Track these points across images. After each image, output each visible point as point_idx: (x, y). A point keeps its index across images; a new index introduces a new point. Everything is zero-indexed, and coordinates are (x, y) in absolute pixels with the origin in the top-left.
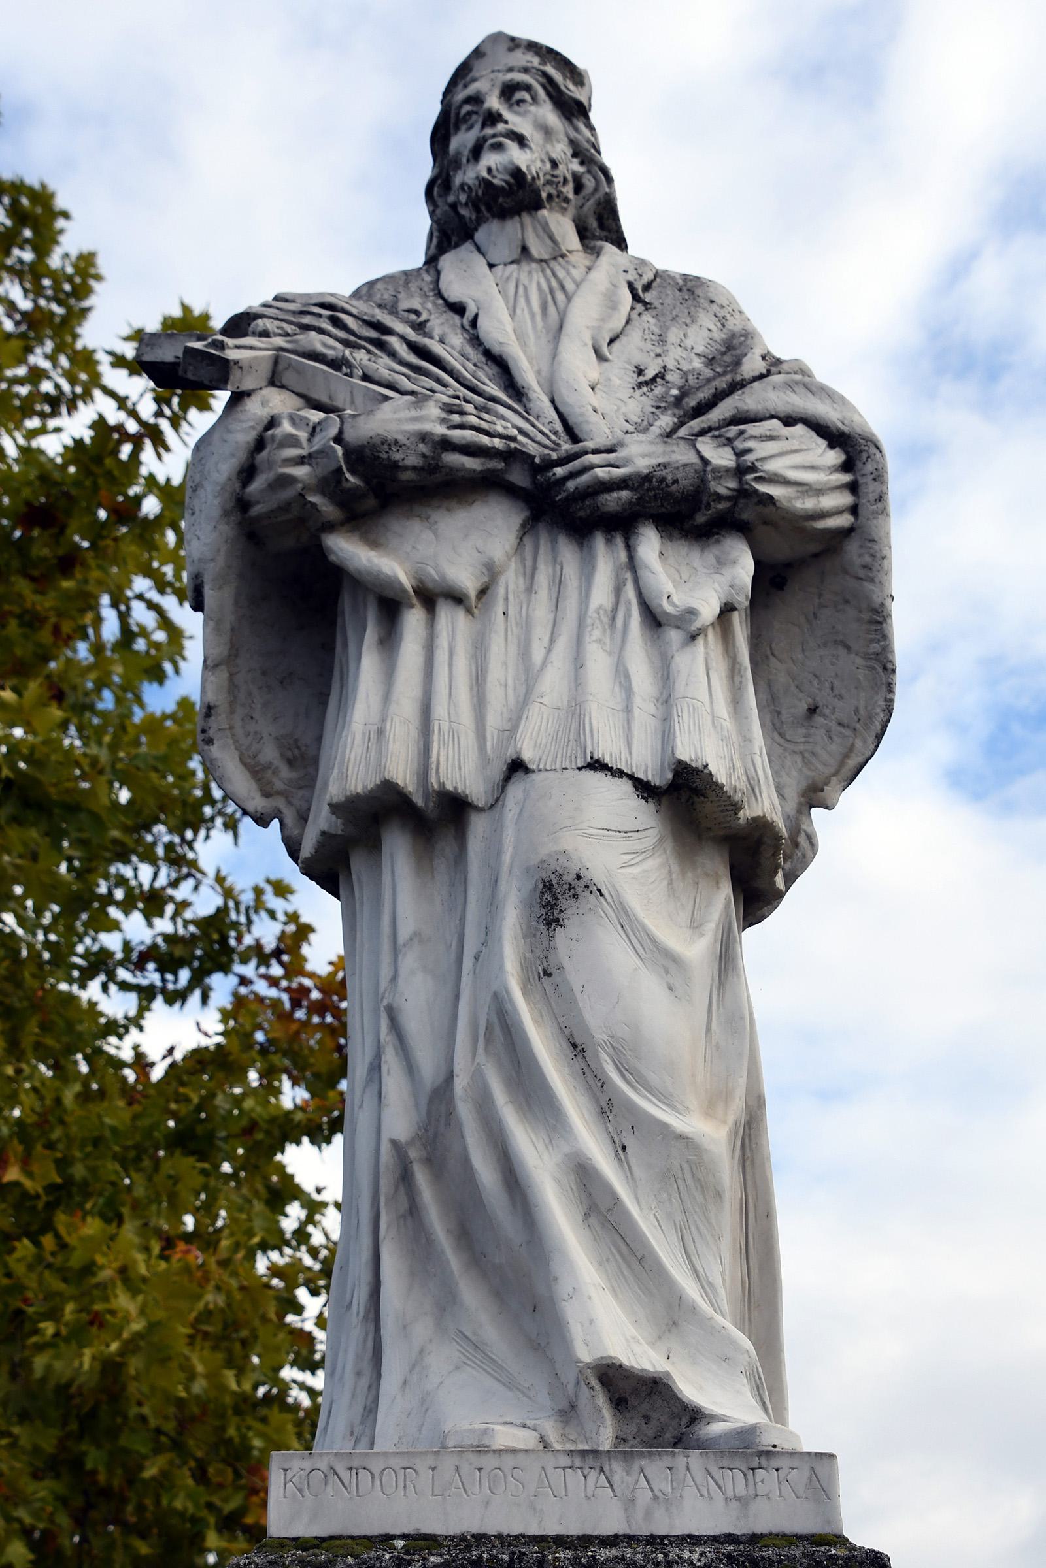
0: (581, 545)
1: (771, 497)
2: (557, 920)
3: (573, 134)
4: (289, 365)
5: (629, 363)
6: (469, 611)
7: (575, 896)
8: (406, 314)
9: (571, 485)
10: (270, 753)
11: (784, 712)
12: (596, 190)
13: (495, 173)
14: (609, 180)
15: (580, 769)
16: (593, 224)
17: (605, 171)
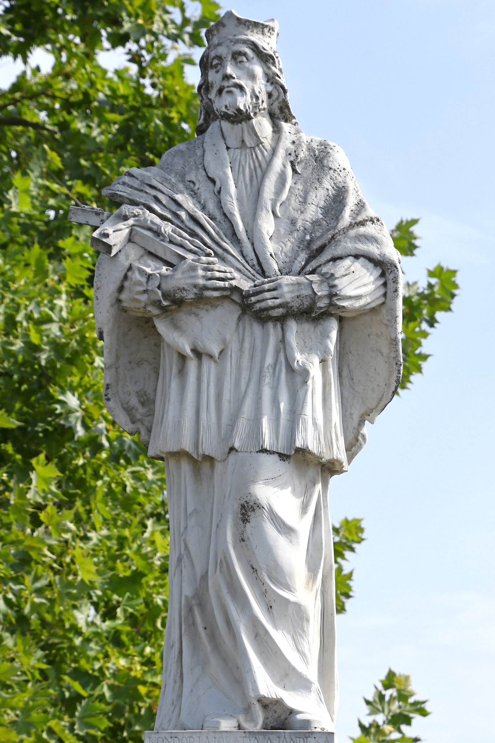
0: (263, 326)
1: (344, 307)
2: (247, 520)
3: (267, 71)
4: (138, 232)
5: (288, 219)
6: (215, 361)
7: (254, 510)
8: (188, 183)
9: (258, 306)
10: (134, 401)
11: (354, 379)
12: (278, 96)
13: (228, 108)
14: (285, 91)
15: (257, 452)
16: (277, 111)
17: (282, 87)
